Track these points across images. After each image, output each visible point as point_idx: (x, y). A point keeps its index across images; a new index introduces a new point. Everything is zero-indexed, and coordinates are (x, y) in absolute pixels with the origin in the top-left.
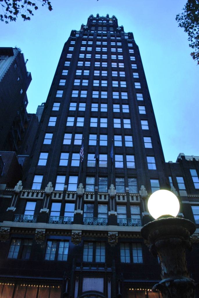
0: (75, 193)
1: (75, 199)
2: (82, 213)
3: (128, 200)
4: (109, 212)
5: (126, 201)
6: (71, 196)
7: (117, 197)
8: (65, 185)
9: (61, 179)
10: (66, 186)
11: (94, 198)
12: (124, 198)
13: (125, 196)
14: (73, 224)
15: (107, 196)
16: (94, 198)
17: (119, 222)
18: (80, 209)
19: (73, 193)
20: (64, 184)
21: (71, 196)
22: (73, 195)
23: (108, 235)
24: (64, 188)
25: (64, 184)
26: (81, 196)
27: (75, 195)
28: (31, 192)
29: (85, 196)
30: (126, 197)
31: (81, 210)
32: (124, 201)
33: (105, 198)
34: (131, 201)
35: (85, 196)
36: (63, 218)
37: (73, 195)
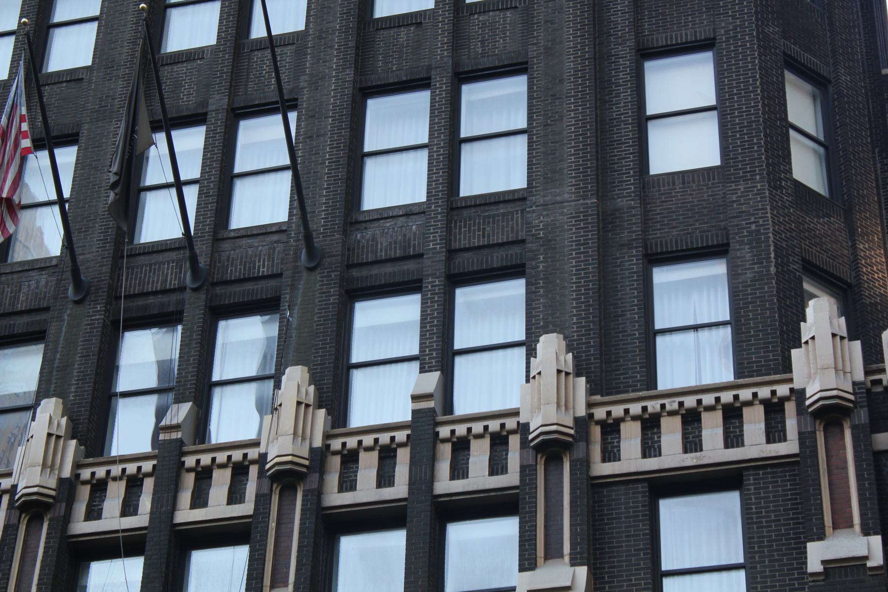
0: (511, 423)
3: (422, 477)
5: (399, 489)
6: (479, 455)
8: (422, 370)
9: (385, 325)
10: (181, 412)
11: (146, 503)
13: (402, 445)
16: (146, 503)
19: (384, 438)
20: (416, 365)
21: (479, 455)
22: (499, 441)
24: (415, 398)
25: (416, 365)
26: (47, 507)
28: (222, 466)
30: (403, 456)
32: (388, 493)
37: (499, 441)
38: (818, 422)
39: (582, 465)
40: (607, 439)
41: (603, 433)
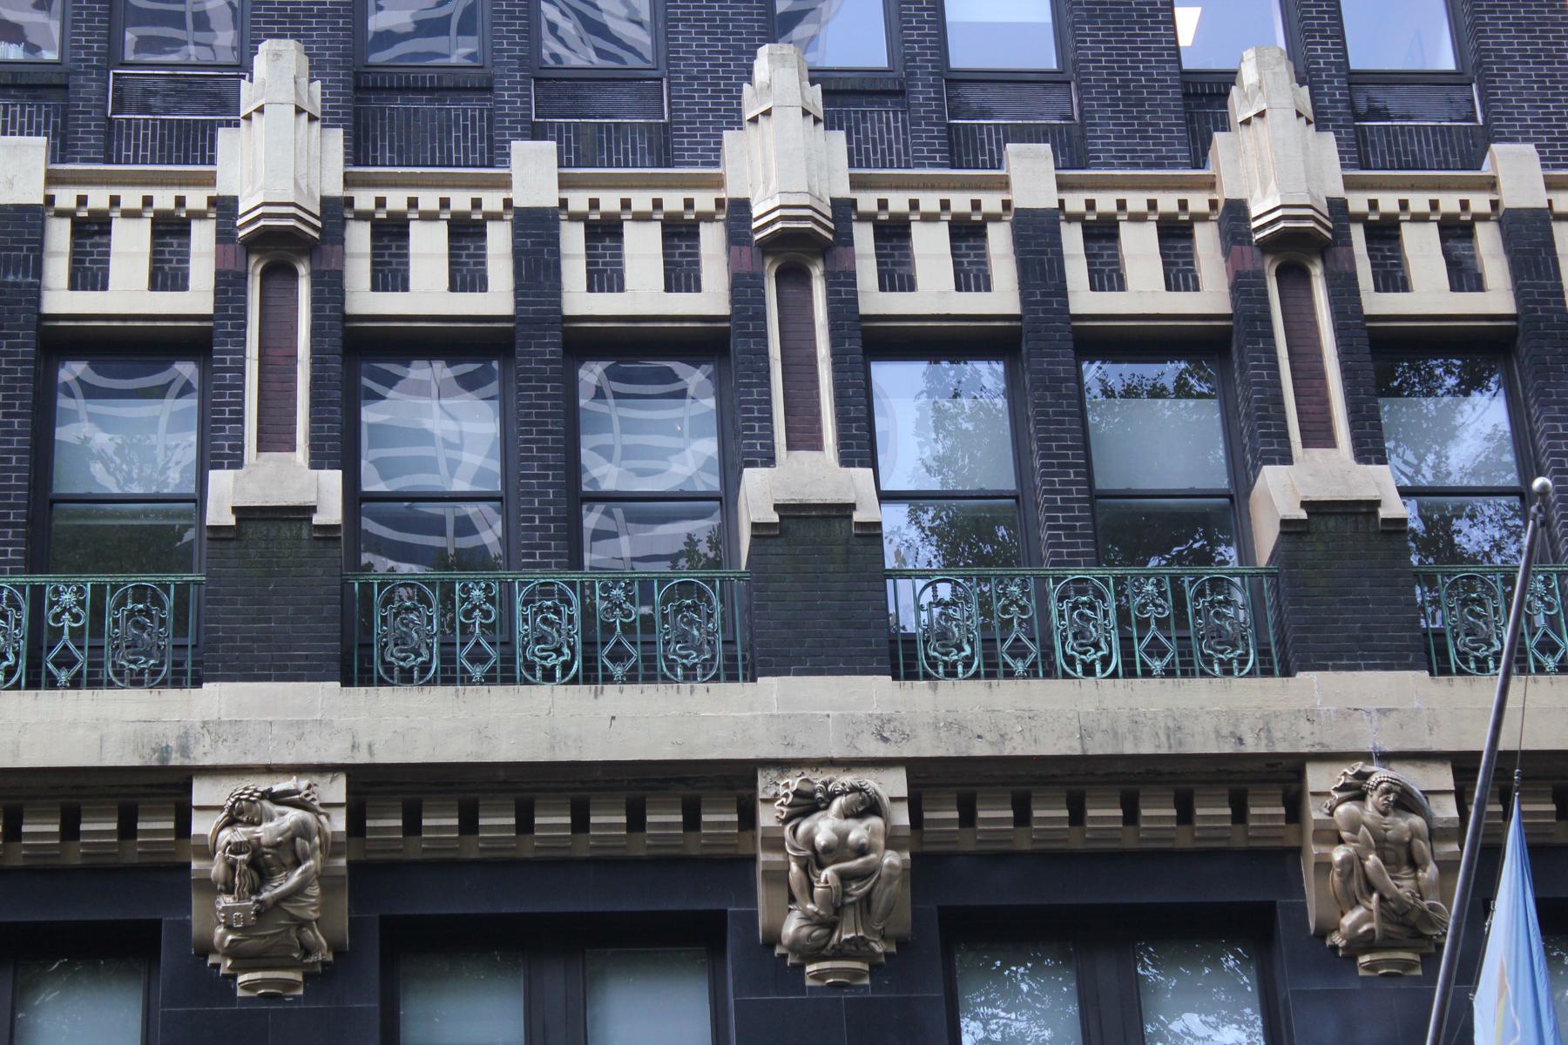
1: (197, 298)
2: (331, 512)
4: (1270, 476)
7: (863, 236)
12: (1189, 256)
14: (197, 683)
15: (712, 239)
17: (909, 623)
18: (816, 444)
23: (748, 818)
27: (203, 236)
29: (359, 237)
31: (318, 460)
33: (681, 275)
34: (1084, 300)
35: (359, 237)
36: (586, 589)
38: (768, 261)
39: (330, 287)
40: (84, 245)
41: (376, 235)
